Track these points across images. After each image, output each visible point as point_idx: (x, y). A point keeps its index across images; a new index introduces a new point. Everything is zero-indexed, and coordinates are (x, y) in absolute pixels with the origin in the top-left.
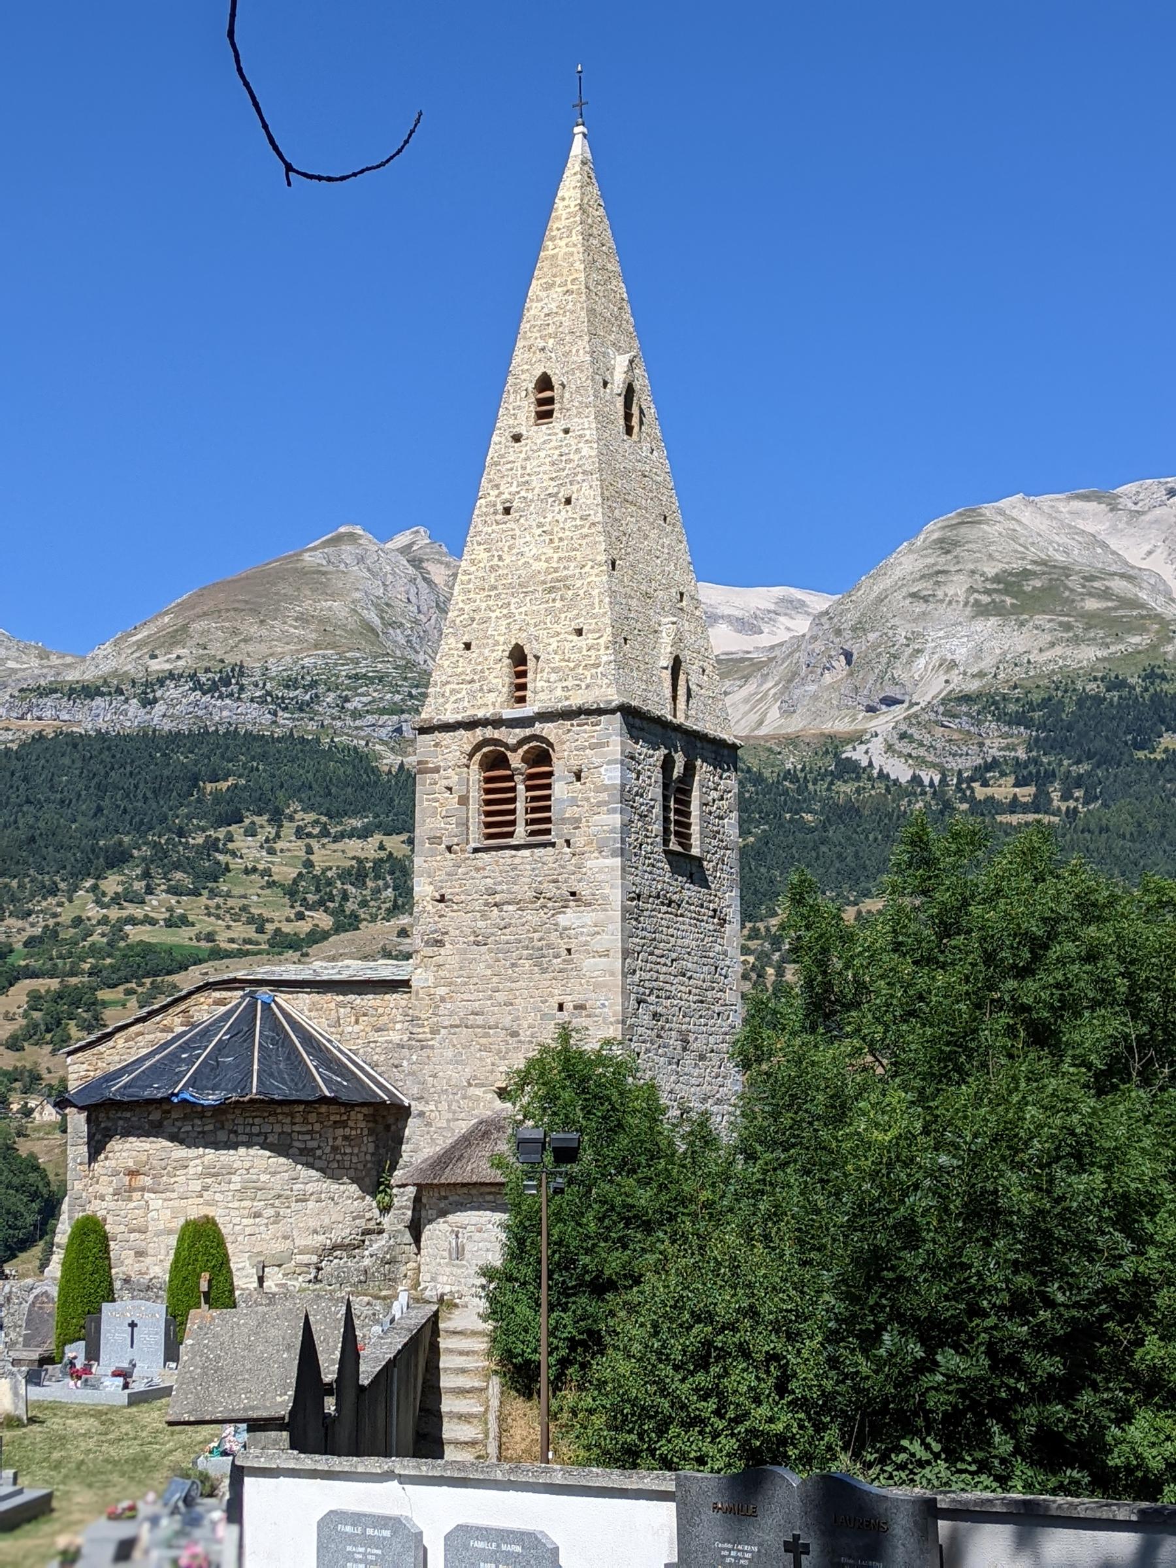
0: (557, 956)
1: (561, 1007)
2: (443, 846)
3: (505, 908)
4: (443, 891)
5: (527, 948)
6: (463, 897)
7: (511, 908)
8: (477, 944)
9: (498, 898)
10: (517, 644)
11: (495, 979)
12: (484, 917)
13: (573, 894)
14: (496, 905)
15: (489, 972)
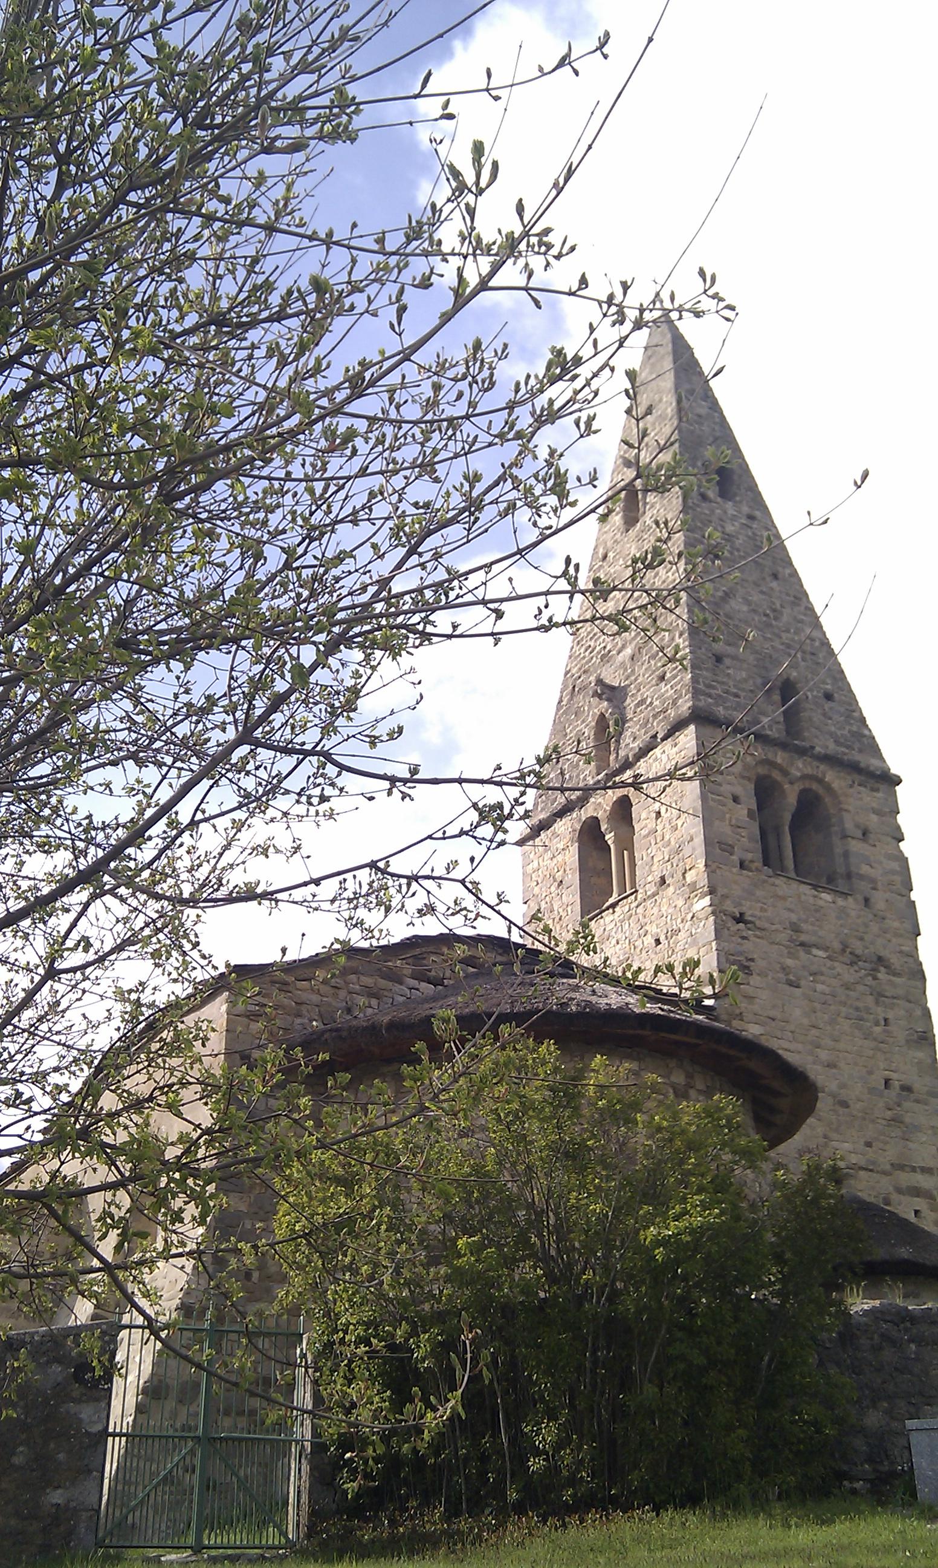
0: (877, 1024)
1: (887, 1082)
2: (735, 858)
3: (815, 951)
4: (744, 909)
5: (844, 1004)
6: (767, 925)
7: (821, 953)
8: (791, 984)
9: (803, 938)
10: (788, 679)
11: (814, 1032)
12: (791, 955)
13: (880, 959)
14: (802, 944)
15: (806, 1021)
